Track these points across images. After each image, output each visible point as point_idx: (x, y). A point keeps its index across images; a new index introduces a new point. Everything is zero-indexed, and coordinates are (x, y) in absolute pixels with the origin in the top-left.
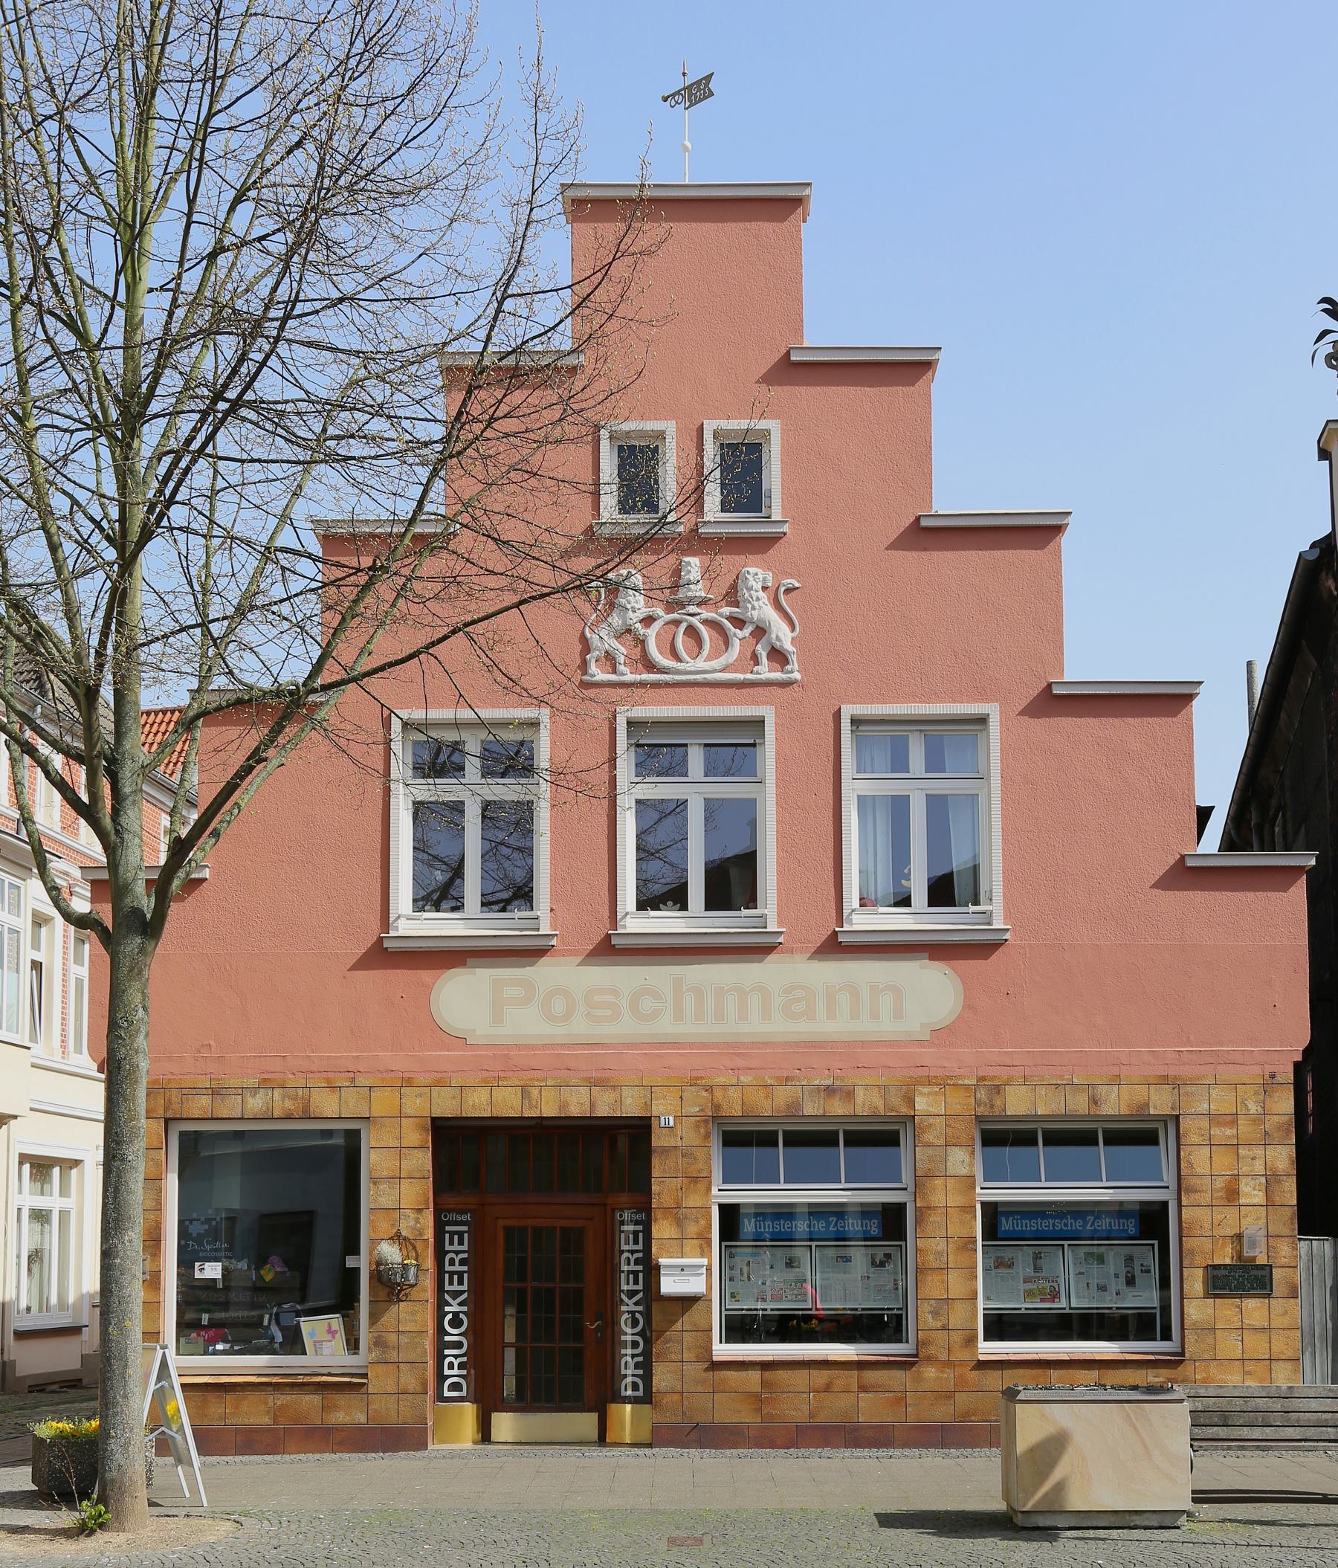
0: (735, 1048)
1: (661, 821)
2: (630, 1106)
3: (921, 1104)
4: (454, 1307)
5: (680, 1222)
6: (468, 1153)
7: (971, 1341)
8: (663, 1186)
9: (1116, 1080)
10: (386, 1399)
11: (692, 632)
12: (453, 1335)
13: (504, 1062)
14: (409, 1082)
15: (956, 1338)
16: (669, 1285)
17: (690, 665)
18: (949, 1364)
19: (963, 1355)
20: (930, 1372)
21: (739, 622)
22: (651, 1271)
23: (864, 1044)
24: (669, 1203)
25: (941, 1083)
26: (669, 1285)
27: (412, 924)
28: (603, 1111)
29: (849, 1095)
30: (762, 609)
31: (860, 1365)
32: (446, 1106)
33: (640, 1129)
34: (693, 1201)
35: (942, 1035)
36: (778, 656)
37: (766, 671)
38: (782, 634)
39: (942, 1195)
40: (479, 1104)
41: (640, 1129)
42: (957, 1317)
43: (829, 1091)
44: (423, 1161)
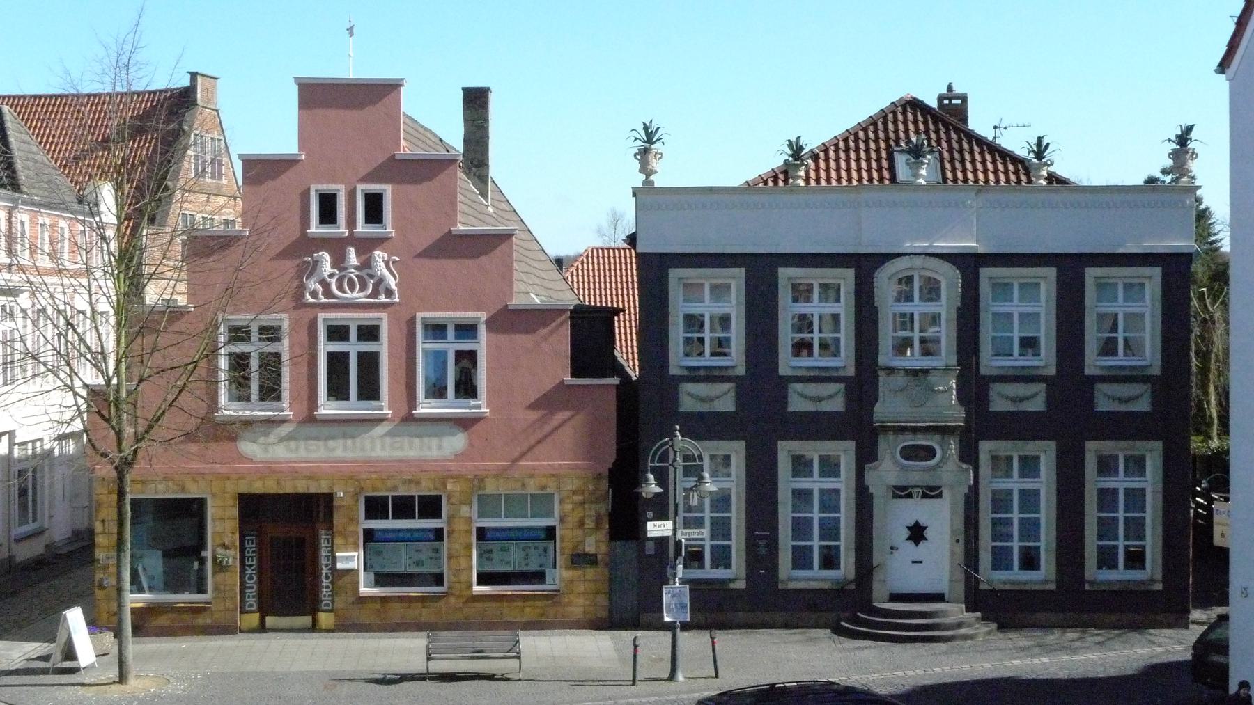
0: (368, 462)
1: (337, 363)
2: (324, 489)
3: (449, 487)
4: (249, 571)
5: (345, 538)
6: (253, 508)
7: (470, 586)
8: (338, 520)
9: (532, 476)
10: (218, 614)
11: (350, 280)
12: (250, 583)
13: (270, 469)
14: (228, 478)
15: (464, 586)
16: (340, 566)
17: (349, 295)
18: (459, 597)
19: (465, 593)
20: (452, 600)
21: (372, 276)
22: (334, 559)
23: (425, 461)
24: (340, 528)
25: (457, 477)
26: (340, 566)
27: (228, 408)
28: (313, 490)
29: (418, 483)
30: (381, 269)
31: (423, 599)
32: (244, 488)
33: (329, 497)
34: (351, 528)
35: (460, 456)
36: (389, 293)
37: (383, 299)
38: (392, 283)
39: (459, 526)
40: (258, 487)
41: (329, 497)
42: (464, 577)
43: (410, 482)
44: (236, 512)
